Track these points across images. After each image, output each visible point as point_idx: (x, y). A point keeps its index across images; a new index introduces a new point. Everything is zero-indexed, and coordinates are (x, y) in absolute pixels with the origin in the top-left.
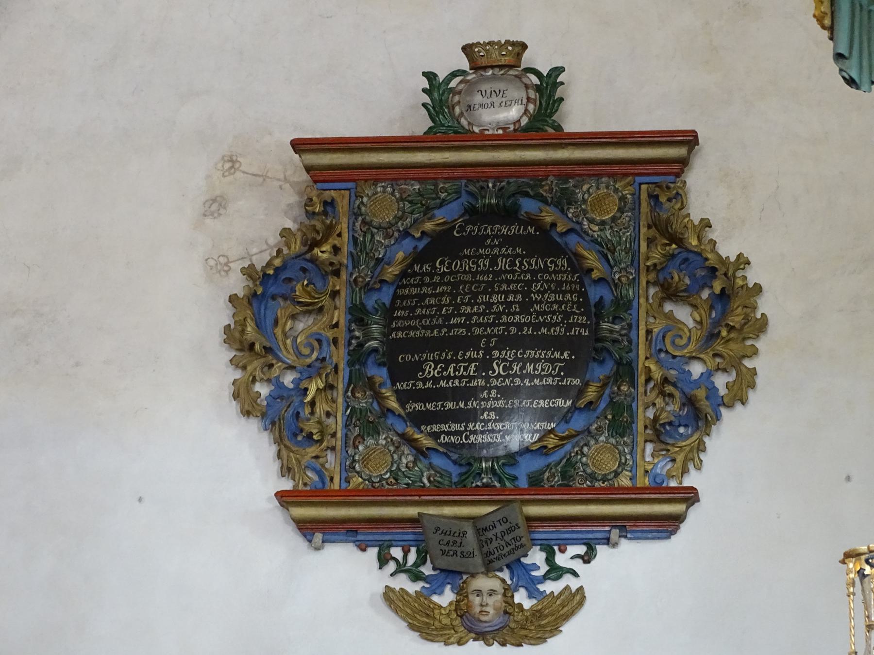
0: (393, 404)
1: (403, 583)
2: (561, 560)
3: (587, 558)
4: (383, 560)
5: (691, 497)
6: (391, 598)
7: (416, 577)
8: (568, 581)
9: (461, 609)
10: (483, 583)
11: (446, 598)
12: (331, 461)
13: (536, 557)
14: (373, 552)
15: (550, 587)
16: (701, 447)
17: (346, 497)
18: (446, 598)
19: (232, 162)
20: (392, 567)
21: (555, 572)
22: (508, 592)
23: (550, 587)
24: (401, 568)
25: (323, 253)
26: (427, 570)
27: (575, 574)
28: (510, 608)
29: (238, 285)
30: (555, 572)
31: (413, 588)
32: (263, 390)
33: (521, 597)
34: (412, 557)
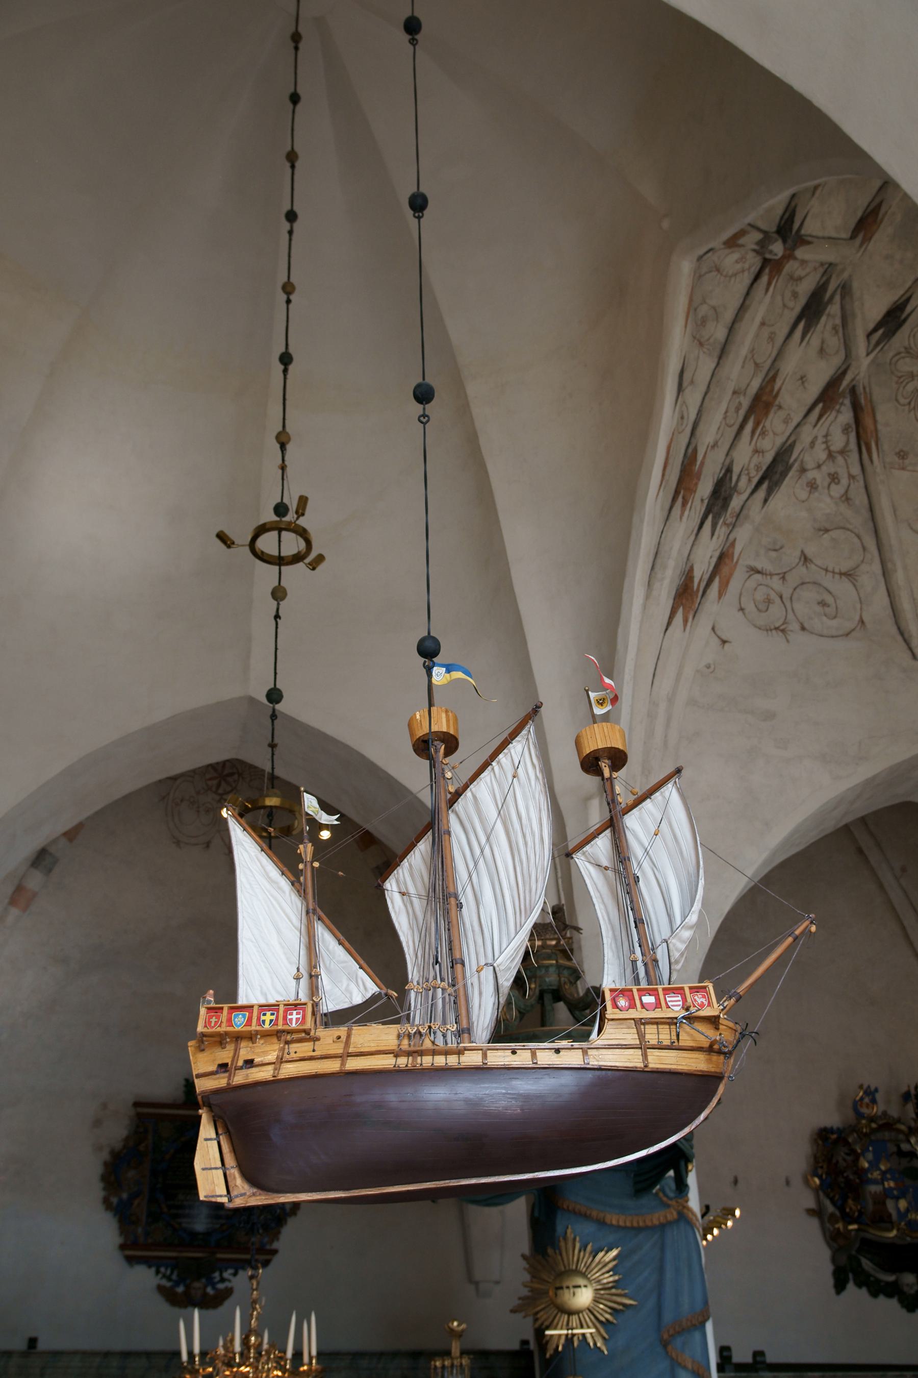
0: (165, 1210)
1: (165, 1282)
2: (226, 1275)
3: (235, 1274)
4: (158, 1272)
5: (275, 1252)
6: (160, 1289)
7: (169, 1279)
8: (227, 1284)
9: (186, 1293)
10: (197, 1285)
11: (180, 1289)
12: (140, 1230)
13: (217, 1275)
14: (153, 1270)
15: (221, 1286)
16: (279, 1232)
17: (146, 1247)
18: (180, 1289)
19: (104, 1106)
20: (160, 1276)
21: (223, 1280)
22: (205, 1287)
23: (221, 1286)
24: (164, 1276)
25: (142, 1148)
26: (174, 1277)
27: (229, 1281)
28: (205, 1294)
29: (105, 1155)
30: (223, 1280)
31: (168, 1284)
32: (115, 1200)
33: (210, 1290)
34: (169, 1272)
